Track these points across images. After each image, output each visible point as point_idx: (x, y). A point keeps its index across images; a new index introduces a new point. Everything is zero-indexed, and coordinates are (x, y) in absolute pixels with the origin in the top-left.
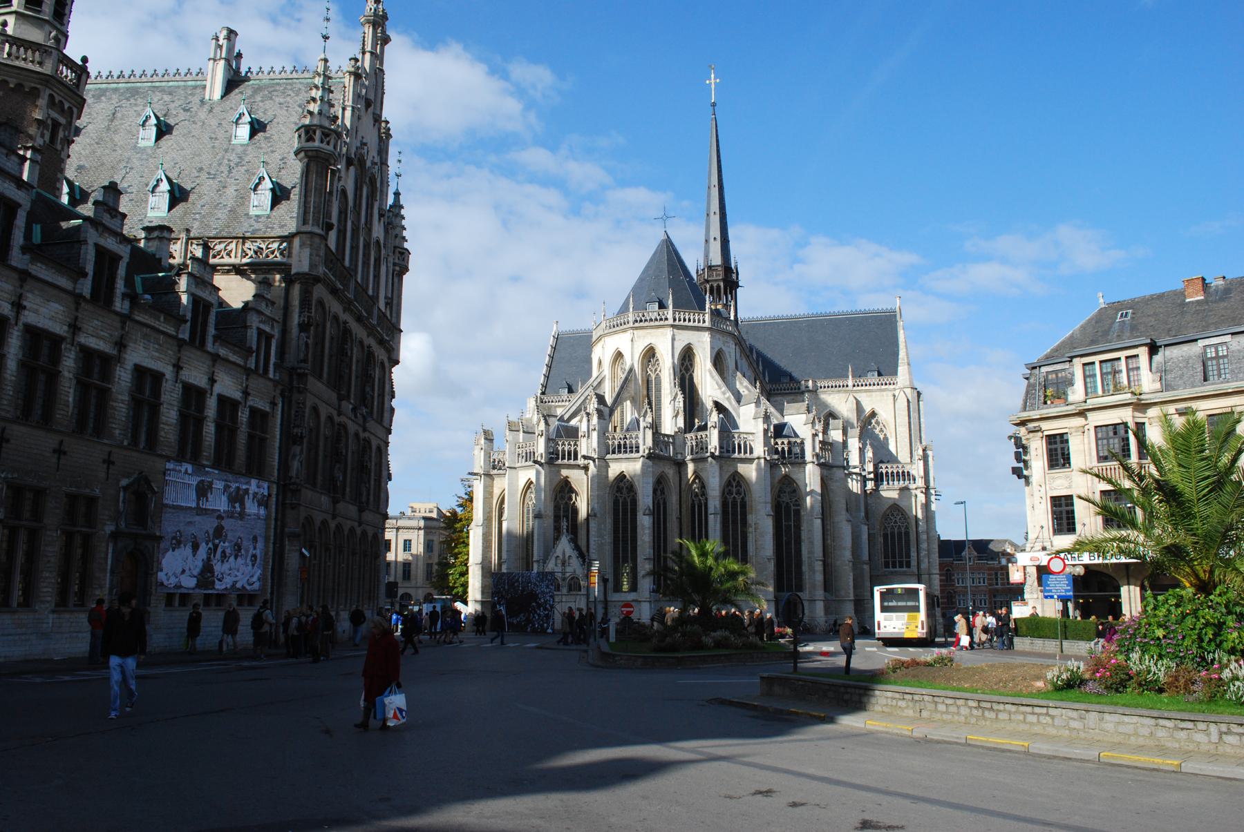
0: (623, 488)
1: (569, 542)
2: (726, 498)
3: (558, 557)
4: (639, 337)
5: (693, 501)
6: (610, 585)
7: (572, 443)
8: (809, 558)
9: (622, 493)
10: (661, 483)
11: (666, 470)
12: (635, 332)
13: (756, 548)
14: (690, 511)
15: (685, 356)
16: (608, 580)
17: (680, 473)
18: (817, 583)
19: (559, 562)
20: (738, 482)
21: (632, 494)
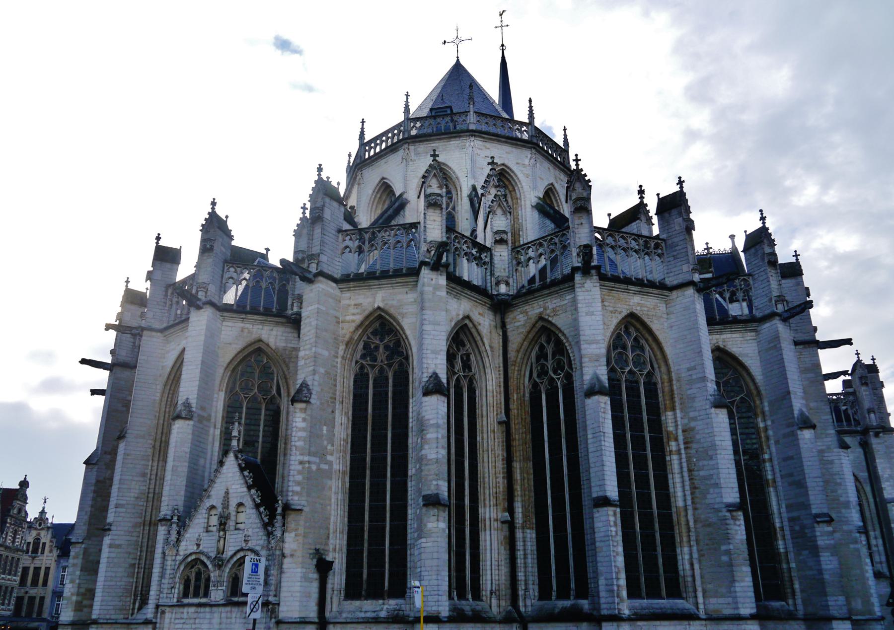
0: (377, 348)
1: (242, 469)
3: (213, 507)
4: (417, 154)
6: (337, 579)
8: (790, 520)
9: (375, 360)
10: (464, 345)
11: (475, 317)
12: (412, 148)
13: (694, 488)
14: (528, 409)
16: (331, 563)
17: (503, 326)
18: (826, 577)
19: (214, 520)
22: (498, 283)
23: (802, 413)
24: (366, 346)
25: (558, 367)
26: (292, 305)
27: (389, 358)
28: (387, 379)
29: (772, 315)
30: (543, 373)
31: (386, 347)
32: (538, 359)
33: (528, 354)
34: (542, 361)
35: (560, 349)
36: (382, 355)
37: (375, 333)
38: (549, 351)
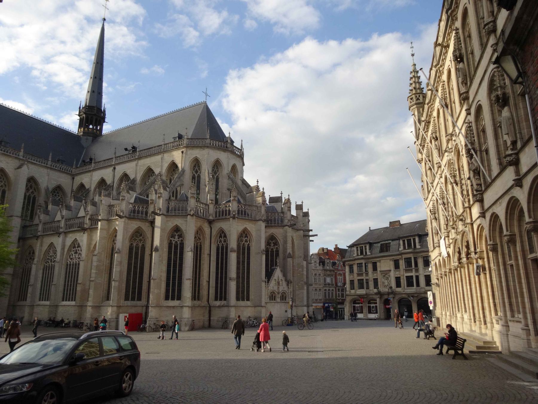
0: (175, 235)
2: (239, 243)
5: (218, 245)
7: (145, 207)
9: (175, 238)
15: (214, 166)
20: (246, 234)
21: (180, 239)
22: (210, 216)
23: (290, 253)
24: (172, 235)
25: (225, 241)
26: (149, 216)
27: (178, 238)
28: (178, 244)
29: (286, 226)
30: (221, 241)
31: (178, 235)
32: (219, 238)
33: (217, 236)
34: (221, 239)
35: (225, 236)
36: (177, 237)
37: (175, 231)
38: (223, 235)
